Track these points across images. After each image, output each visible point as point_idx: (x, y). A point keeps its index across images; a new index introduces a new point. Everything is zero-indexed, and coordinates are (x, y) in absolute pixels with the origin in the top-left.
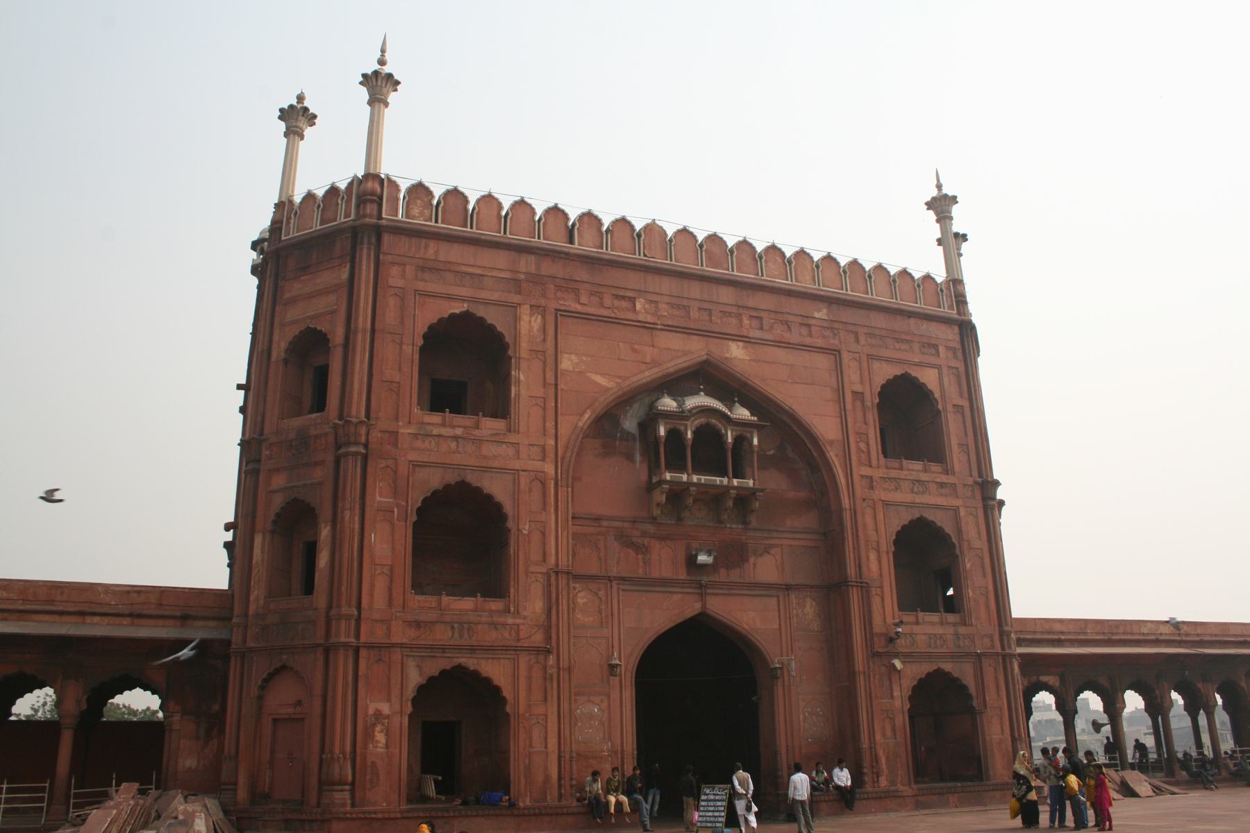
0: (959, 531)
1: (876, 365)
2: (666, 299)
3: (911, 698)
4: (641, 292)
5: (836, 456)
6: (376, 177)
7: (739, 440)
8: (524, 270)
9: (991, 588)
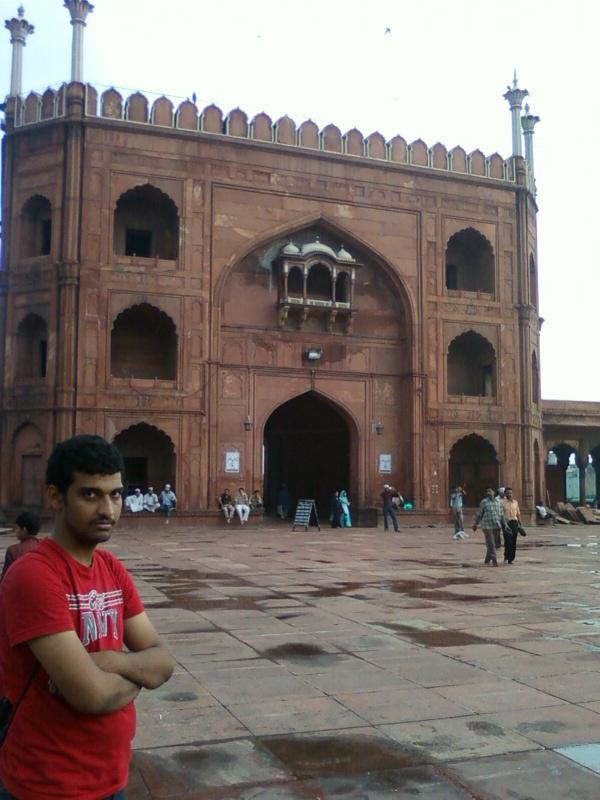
0: (499, 341)
1: (448, 222)
2: (294, 174)
5: (412, 287)
6: (82, 86)
7: (343, 276)
8: (188, 154)
9: (518, 381)
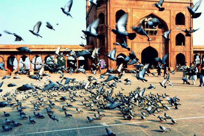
1: (176, 11)
3: (176, 57)
4: (143, 4)
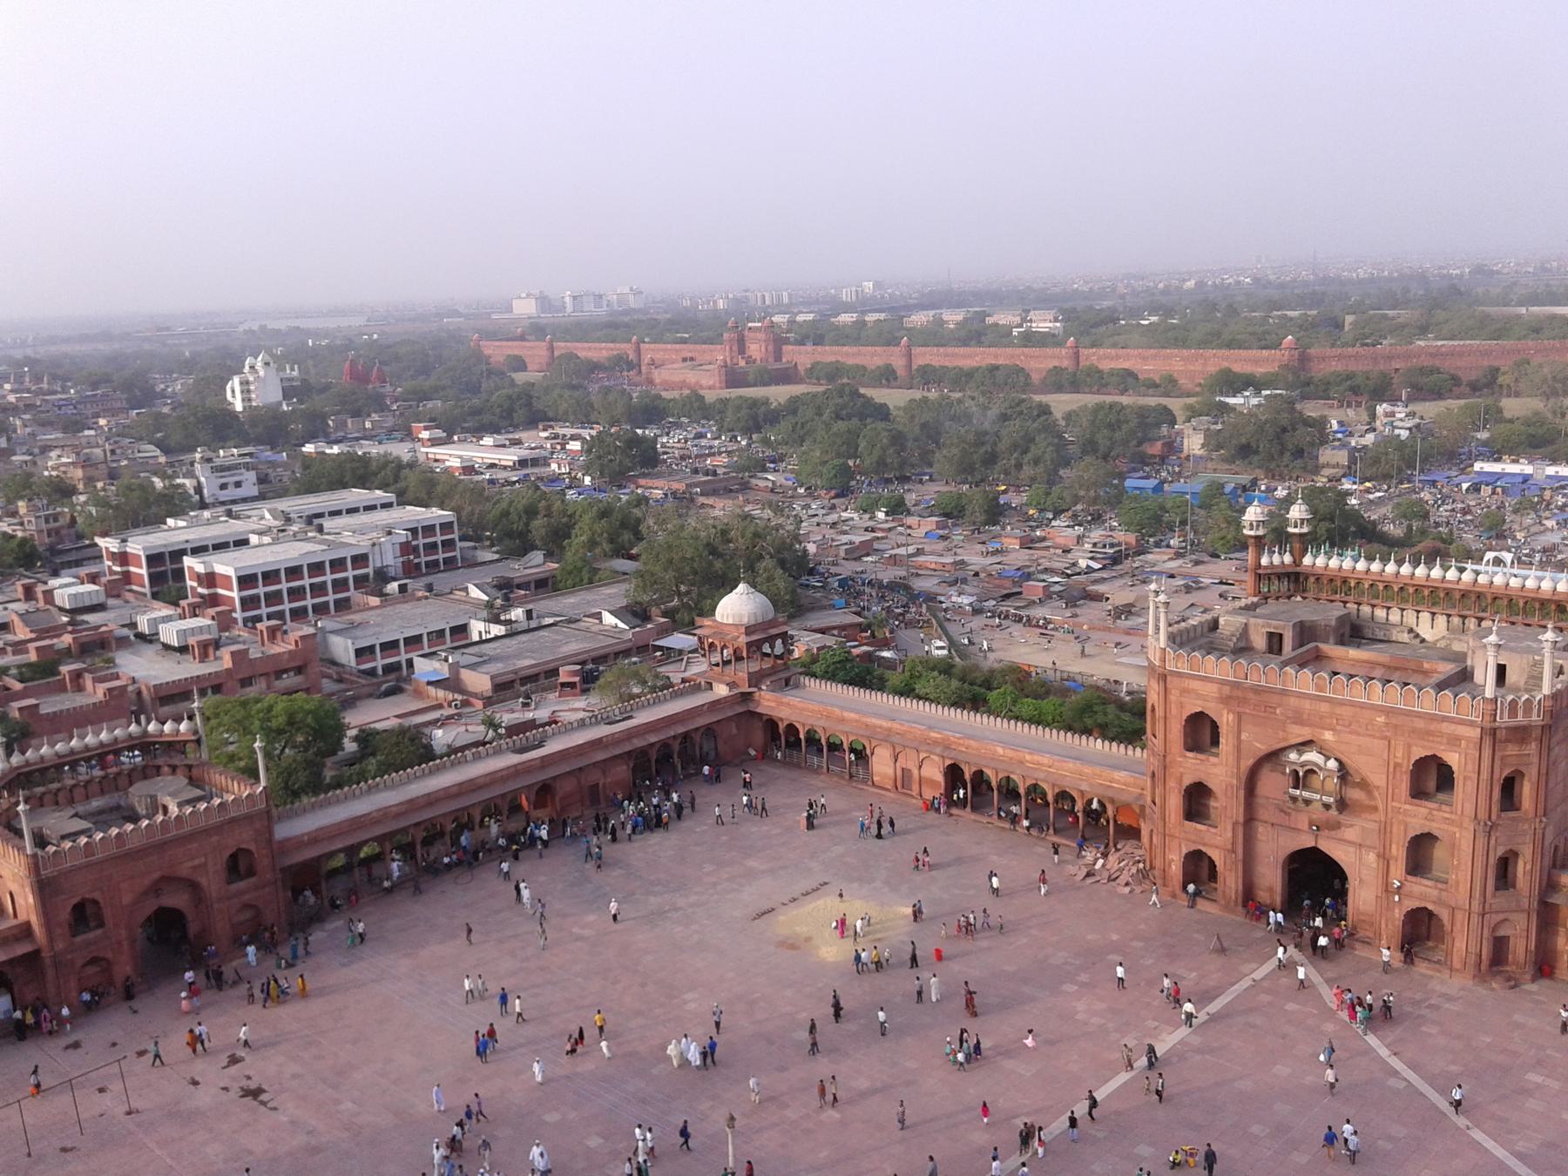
9: (1469, 878)
